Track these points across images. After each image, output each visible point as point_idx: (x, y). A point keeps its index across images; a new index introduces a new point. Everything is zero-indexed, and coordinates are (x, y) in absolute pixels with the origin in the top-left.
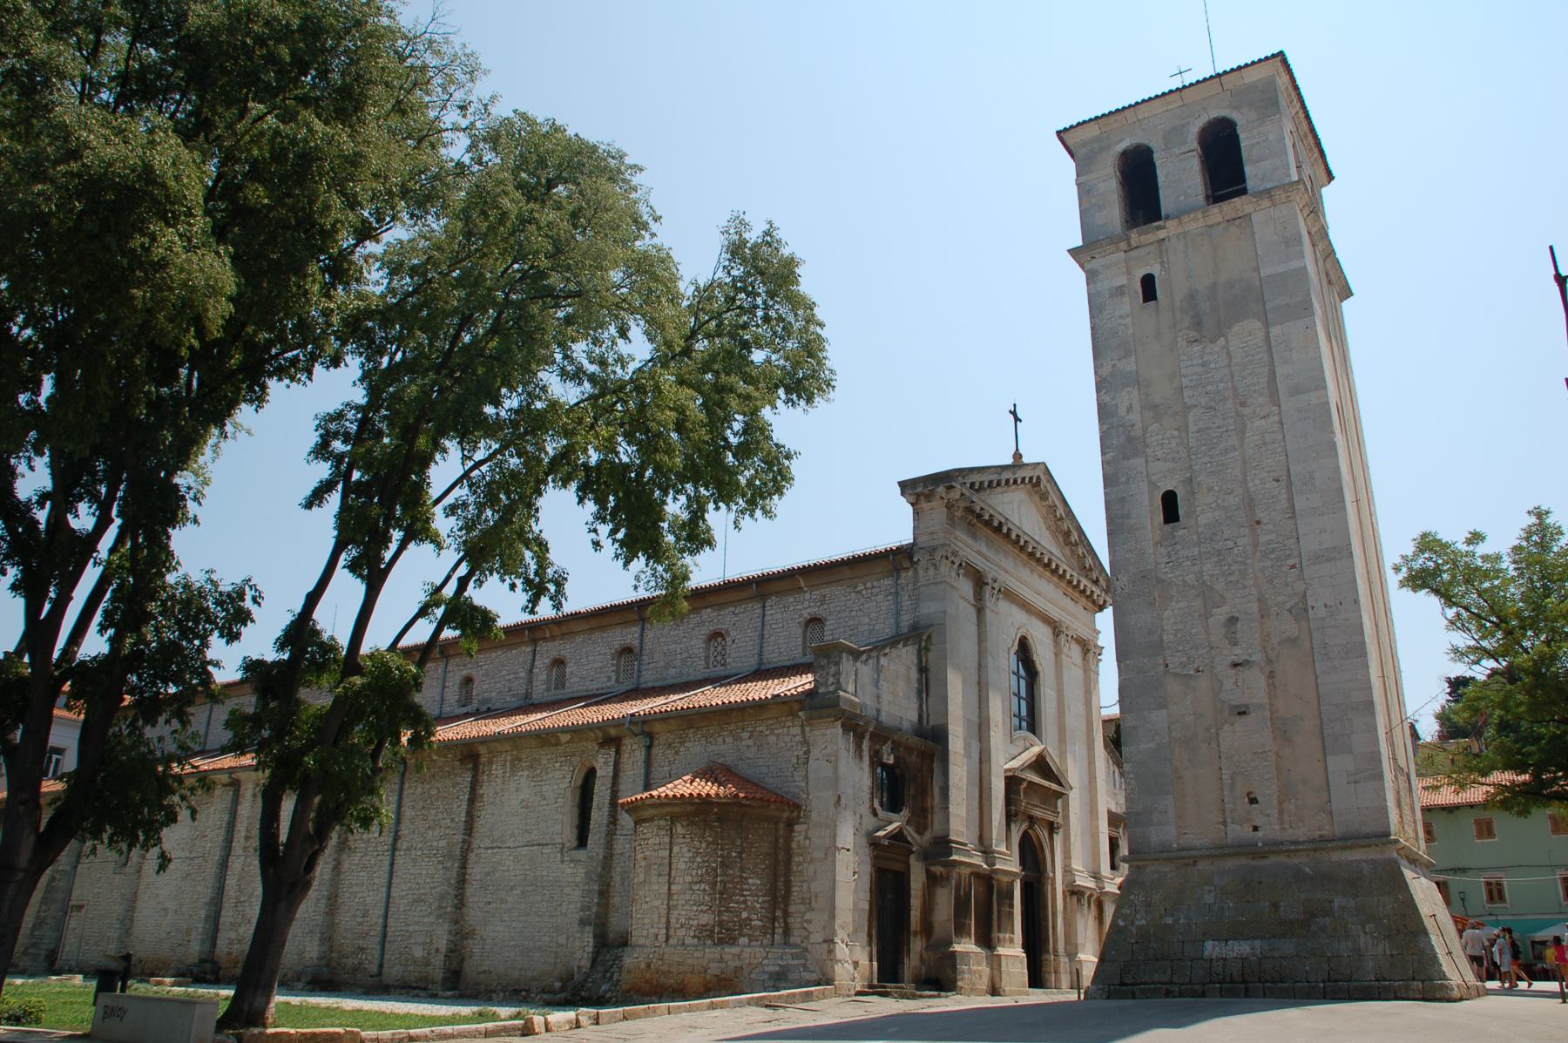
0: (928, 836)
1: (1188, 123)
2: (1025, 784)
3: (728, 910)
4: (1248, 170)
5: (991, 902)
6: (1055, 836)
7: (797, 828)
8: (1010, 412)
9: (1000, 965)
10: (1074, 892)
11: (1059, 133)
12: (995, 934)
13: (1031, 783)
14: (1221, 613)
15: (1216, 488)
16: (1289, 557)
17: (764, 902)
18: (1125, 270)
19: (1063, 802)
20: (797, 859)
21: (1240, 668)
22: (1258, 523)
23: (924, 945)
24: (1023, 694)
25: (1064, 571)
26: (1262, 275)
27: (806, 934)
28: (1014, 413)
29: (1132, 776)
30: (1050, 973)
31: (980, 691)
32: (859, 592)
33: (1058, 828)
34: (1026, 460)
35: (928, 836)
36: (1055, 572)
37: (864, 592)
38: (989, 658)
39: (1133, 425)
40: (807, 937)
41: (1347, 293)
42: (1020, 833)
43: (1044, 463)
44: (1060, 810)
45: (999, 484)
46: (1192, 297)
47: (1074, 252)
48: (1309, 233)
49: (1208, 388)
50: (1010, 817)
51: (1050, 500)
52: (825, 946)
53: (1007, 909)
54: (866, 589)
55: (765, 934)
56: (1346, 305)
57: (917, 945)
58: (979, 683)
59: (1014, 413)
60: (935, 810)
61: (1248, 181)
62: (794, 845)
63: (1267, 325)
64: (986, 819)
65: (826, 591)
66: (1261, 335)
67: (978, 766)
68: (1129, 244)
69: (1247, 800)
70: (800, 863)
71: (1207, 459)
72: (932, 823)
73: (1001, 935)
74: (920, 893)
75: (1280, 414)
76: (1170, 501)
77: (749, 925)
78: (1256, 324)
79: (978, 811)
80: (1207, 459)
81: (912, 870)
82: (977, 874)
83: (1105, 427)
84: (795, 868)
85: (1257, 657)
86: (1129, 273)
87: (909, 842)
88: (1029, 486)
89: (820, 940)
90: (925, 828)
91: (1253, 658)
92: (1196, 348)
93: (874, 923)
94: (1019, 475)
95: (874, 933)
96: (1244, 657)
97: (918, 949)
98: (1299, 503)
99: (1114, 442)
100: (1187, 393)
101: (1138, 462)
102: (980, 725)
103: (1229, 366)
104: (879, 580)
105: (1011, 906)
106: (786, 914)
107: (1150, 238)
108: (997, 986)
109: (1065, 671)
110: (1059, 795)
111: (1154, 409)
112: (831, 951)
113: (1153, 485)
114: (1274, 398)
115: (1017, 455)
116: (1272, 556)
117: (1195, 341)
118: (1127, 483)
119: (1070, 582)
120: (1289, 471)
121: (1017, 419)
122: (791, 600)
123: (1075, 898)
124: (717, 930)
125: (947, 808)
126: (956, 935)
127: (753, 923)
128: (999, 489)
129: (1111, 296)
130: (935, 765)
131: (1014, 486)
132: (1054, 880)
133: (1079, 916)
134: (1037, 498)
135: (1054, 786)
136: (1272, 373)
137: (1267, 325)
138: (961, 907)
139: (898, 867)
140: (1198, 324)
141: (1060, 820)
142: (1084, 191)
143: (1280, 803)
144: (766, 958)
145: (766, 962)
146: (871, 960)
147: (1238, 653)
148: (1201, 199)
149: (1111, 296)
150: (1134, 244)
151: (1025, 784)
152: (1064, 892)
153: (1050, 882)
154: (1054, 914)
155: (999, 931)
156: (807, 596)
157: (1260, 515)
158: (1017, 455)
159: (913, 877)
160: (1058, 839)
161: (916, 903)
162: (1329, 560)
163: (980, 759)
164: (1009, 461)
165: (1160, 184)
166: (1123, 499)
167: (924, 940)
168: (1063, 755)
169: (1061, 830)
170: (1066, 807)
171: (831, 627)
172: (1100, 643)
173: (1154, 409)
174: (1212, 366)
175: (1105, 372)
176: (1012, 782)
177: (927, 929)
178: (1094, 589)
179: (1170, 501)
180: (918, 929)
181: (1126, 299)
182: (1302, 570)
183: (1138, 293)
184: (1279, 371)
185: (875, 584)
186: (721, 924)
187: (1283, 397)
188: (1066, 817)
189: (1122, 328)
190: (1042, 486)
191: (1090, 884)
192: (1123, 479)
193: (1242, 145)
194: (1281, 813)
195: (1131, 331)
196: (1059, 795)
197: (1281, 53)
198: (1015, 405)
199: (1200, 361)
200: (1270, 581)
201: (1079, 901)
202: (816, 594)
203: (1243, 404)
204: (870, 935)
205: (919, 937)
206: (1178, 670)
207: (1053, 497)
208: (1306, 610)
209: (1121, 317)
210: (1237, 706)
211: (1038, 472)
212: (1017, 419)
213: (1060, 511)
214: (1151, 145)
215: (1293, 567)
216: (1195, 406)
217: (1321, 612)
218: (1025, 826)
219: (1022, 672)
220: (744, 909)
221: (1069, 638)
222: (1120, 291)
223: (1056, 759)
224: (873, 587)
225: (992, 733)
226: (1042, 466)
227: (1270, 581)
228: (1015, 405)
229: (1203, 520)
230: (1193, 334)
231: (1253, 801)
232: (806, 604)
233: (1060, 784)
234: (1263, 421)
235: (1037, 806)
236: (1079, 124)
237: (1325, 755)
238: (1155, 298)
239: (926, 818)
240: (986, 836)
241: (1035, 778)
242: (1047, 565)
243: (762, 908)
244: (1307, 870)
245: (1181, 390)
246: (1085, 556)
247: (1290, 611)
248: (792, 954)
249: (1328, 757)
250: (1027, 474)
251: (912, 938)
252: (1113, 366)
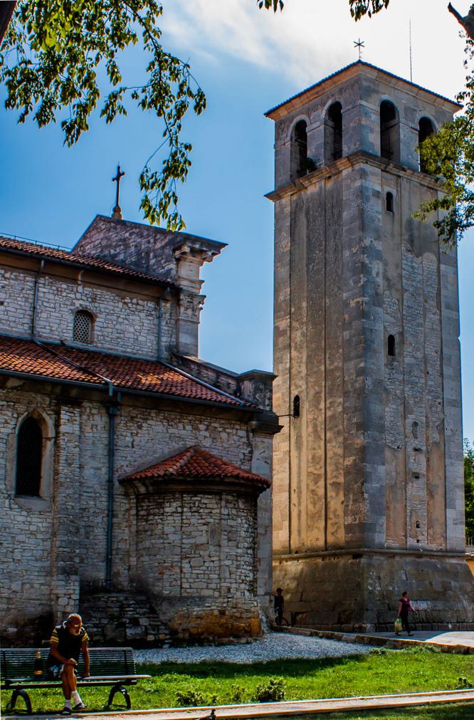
16: (438, 397)
32: (125, 303)
37: (130, 305)
54: (131, 303)
65: (98, 292)
68: (386, 168)
85: (424, 448)
104: (144, 300)
114: (439, 307)
122: (64, 286)
140: (411, 241)
150: (387, 169)
156: (80, 288)
171: (101, 324)
185: (140, 302)
200: (431, 408)
202: (87, 290)
215: (439, 403)
224: (138, 304)
227: (431, 408)
231: (418, 526)
232: (78, 296)
237: (446, 508)
249: (447, 510)
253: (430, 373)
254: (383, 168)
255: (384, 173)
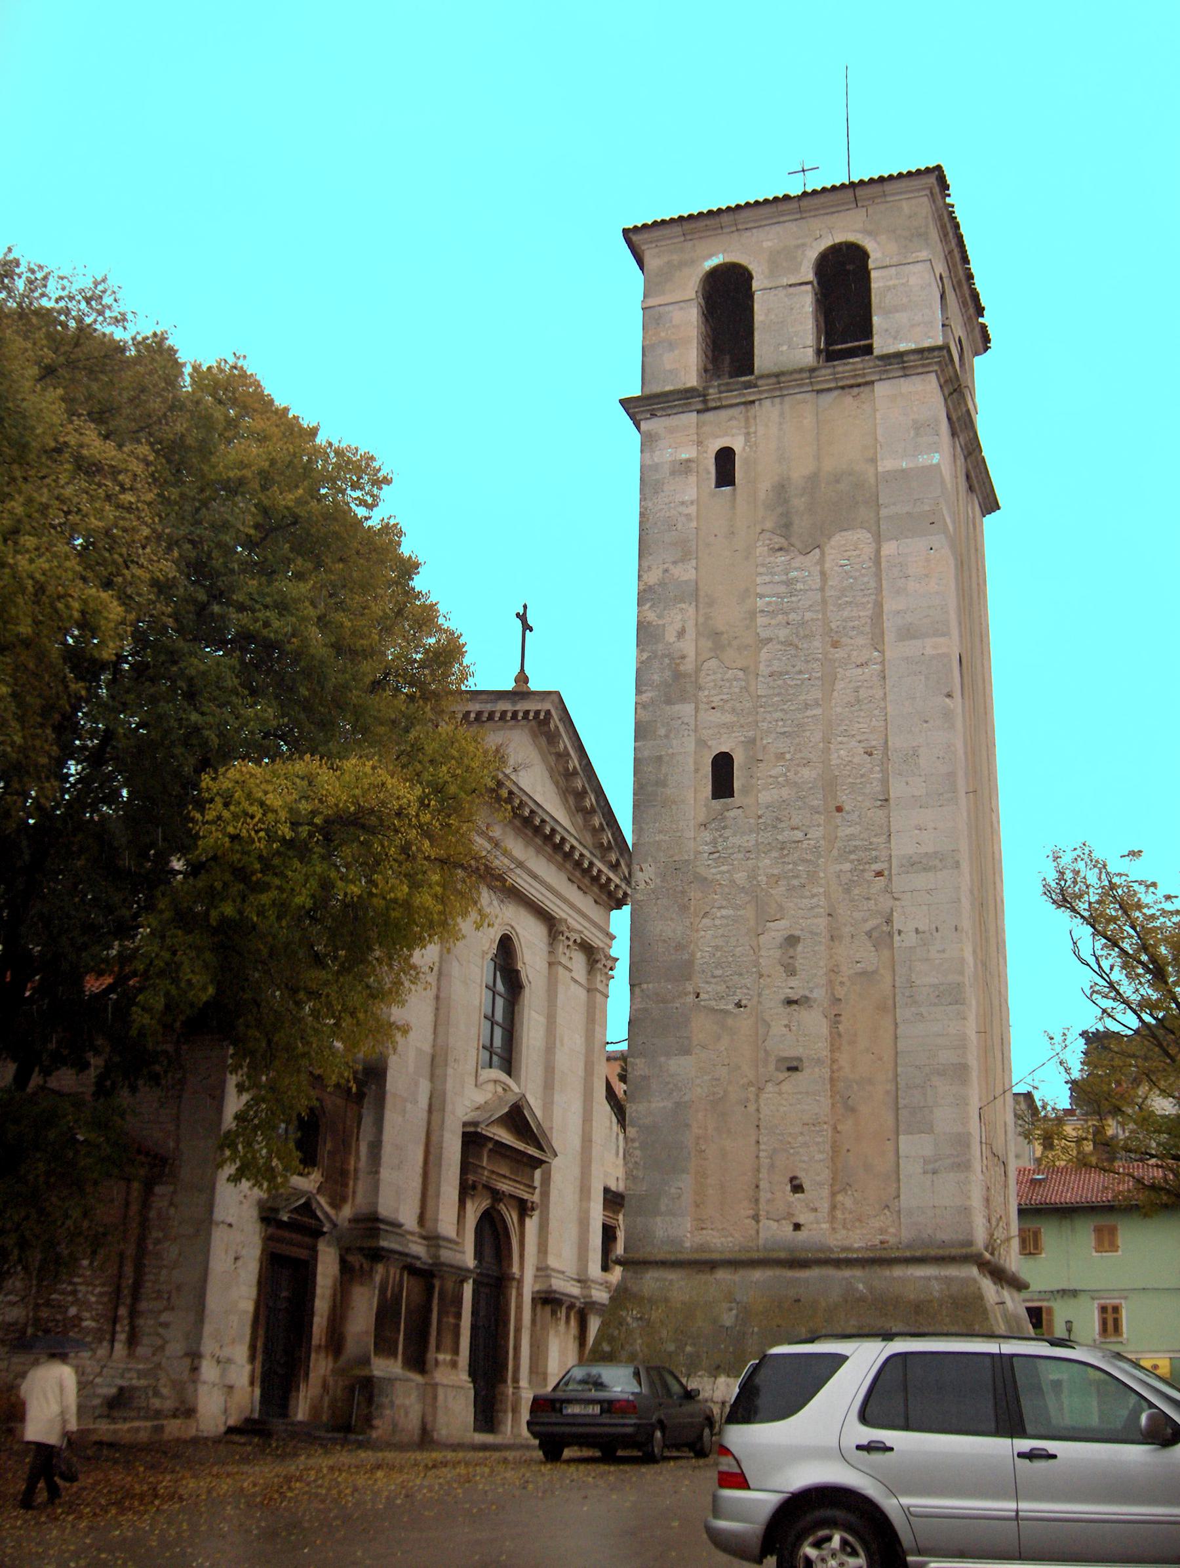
0: (347, 1212)
1: (804, 245)
2: (490, 1146)
3: (48, 1303)
4: (875, 320)
5: (429, 1310)
6: (527, 1220)
7: (158, 1189)
8: (518, 615)
9: (435, 1397)
10: (548, 1300)
11: (626, 232)
12: (431, 1354)
13: (499, 1144)
14: (778, 930)
15: (788, 756)
16: (876, 860)
17: (101, 1294)
18: (695, 437)
19: (543, 1174)
20: (156, 1234)
21: (795, 1007)
22: (839, 809)
23: (330, 1366)
24: (499, 1017)
25: (573, 847)
26: (880, 469)
27: (160, 1342)
28: (522, 617)
29: (637, 1144)
30: (505, 1412)
31: (437, 1009)
33: (533, 1209)
34: (534, 685)
35: (347, 1212)
36: (558, 848)
38: (455, 964)
39: (683, 657)
40: (162, 1348)
41: (990, 504)
42: (479, 1214)
43: (558, 693)
44: (537, 1183)
45: (491, 716)
46: (781, 489)
47: (627, 404)
48: (949, 418)
49: (792, 616)
50: (466, 1190)
51: (562, 746)
52: (187, 1361)
53: (452, 1320)
55: (100, 1341)
56: (989, 521)
57: (320, 1367)
58: (437, 998)
59: (522, 617)
60: (361, 1175)
61: (876, 338)
62: (152, 1214)
63: (878, 539)
64: (431, 1191)
66: (868, 550)
67: (425, 1115)
68: (705, 402)
69: (789, 1188)
70: (158, 1241)
71: (779, 715)
72: (354, 1192)
73: (441, 1357)
74: (328, 1292)
75: (883, 663)
76: (723, 767)
77: (78, 1326)
78: (862, 536)
79: (420, 1180)
80: (779, 715)
81: (320, 1258)
82: (412, 1269)
83: (645, 655)
84: (151, 1247)
85: (819, 994)
86: (699, 443)
87: (318, 1219)
88: (533, 723)
89: (181, 1353)
90: (344, 1199)
91: (815, 995)
92: (781, 558)
93: (261, 1332)
94: (521, 706)
95: (259, 1344)
96: (801, 992)
97: (322, 1372)
98: (897, 789)
99: (656, 677)
100: (761, 620)
101: (687, 709)
102: (433, 1058)
103: (822, 589)
105: (459, 1316)
106: (133, 1314)
107: (733, 398)
108: (429, 1427)
109: (561, 989)
110: (539, 1163)
111: (716, 640)
112: (195, 1369)
113: (701, 743)
114: (877, 641)
115: (522, 678)
116: (852, 857)
117: (781, 549)
118: (667, 736)
119: (578, 864)
120: (886, 742)
121: (527, 627)
123: (548, 1309)
124: (30, 1331)
125: (377, 1172)
126: (376, 1354)
127: (85, 1324)
128: (489, 725)
129: (673, 473)
130: (364, 1111)
131: (513, 722)
132: (520, 1281)
133: (552, 1333)
134: (543, 741)
135: (532, 1151)
136: (879, 605)
137: (878, 539)
138: (386, 1315)
139: (302, 1254)
140: (785, 527)
141: (536, 1198)
142: (652, 317)
143: (833, 1194)
144: (100, 1374)
145: (98, 1380)
146: (252, 1383)
147: (796, 987)
148: (807, 356)
149: (673, 473)
151: (490, 1146)
152: (533, 1299)
153: (515, 1284)
154: (518, 1330)
155: (438, 1349)
157: (844, 798)
158: (522, 678)
159: (320, 1269)
160: (531, 1224)
161: (322, 1306)
162: (926, 869)
163: (430, 1106)
164: (509, 685)
165: (756, 325)
166: (660, 758)
167: (330, 1358)
168: (548, 1105)
169: (536, 1213)
170: (546, 1180)
172: (613, 952)
173: (716, 640)
174: (799, 586)
175: (653, 578)
176: (472, 1140)
177: (336, 1342)
178: (611, 875)
179: (723, 767)
180: (323, 1343)
181: (693, 479)
182: (890, 880)
183: (709, 473)
184: (890, 605)
186: (37, 1321)
187: (889, 637)
188: (545, 1194)
189: (683, 519)
190: (552, 726)
191: (575, 1290)
192: (662, 732)
193: (874, 285)
194: (833, 1207)
195: (694, 524)
196: (539, 1163)
197: (939, 168)
198: (525, 607)
199: (784, 578)
200: (848, 891)
201: (554, 1313)
203: (835, 645)
204: (253, 1347)
205: (323, 1355)
206: (713, 1003)
207: (566, 741)
208: (890, 935)
209: (683, 503)
210: (786, 1059)
211: (547, 706)
212: (527, 627)
213: (574, 762)
214: (750, 267)
215: (879, 874)
216: (770, 640)
217: (911, 939)
218: (485, 1204)
219: (500, 987)
220: (72, 1304)
221: (571, 943)
222: (684, 468)
223: (539, 1113)
225: (450, 1071)
226: (554, 697)
227: (848, 891)
228: (525, 607)
229: (765, 797)
230: (779, 541)
231: (797, 1188)
233: (540, 1148)
234: (860, 671)
235: (504, 1176)
236: (655, 223)
237: (898, 1135)
238: (731, 483)
239: (346, 1185)
240: (429, 1215)
241: (505, 1136)
242: (548, 838)
243: (97, 1302)
244: (861, 1286)
245: (752, 615)
246: (603, 829)
247: (869, 934)
248: (138, 1371)
249: (901, 1137)
250: (532, 706)
251: (313, 1356)
252: (666, 571)
253: (847, 808)
254: (700, 407)
255: (709, 416)
